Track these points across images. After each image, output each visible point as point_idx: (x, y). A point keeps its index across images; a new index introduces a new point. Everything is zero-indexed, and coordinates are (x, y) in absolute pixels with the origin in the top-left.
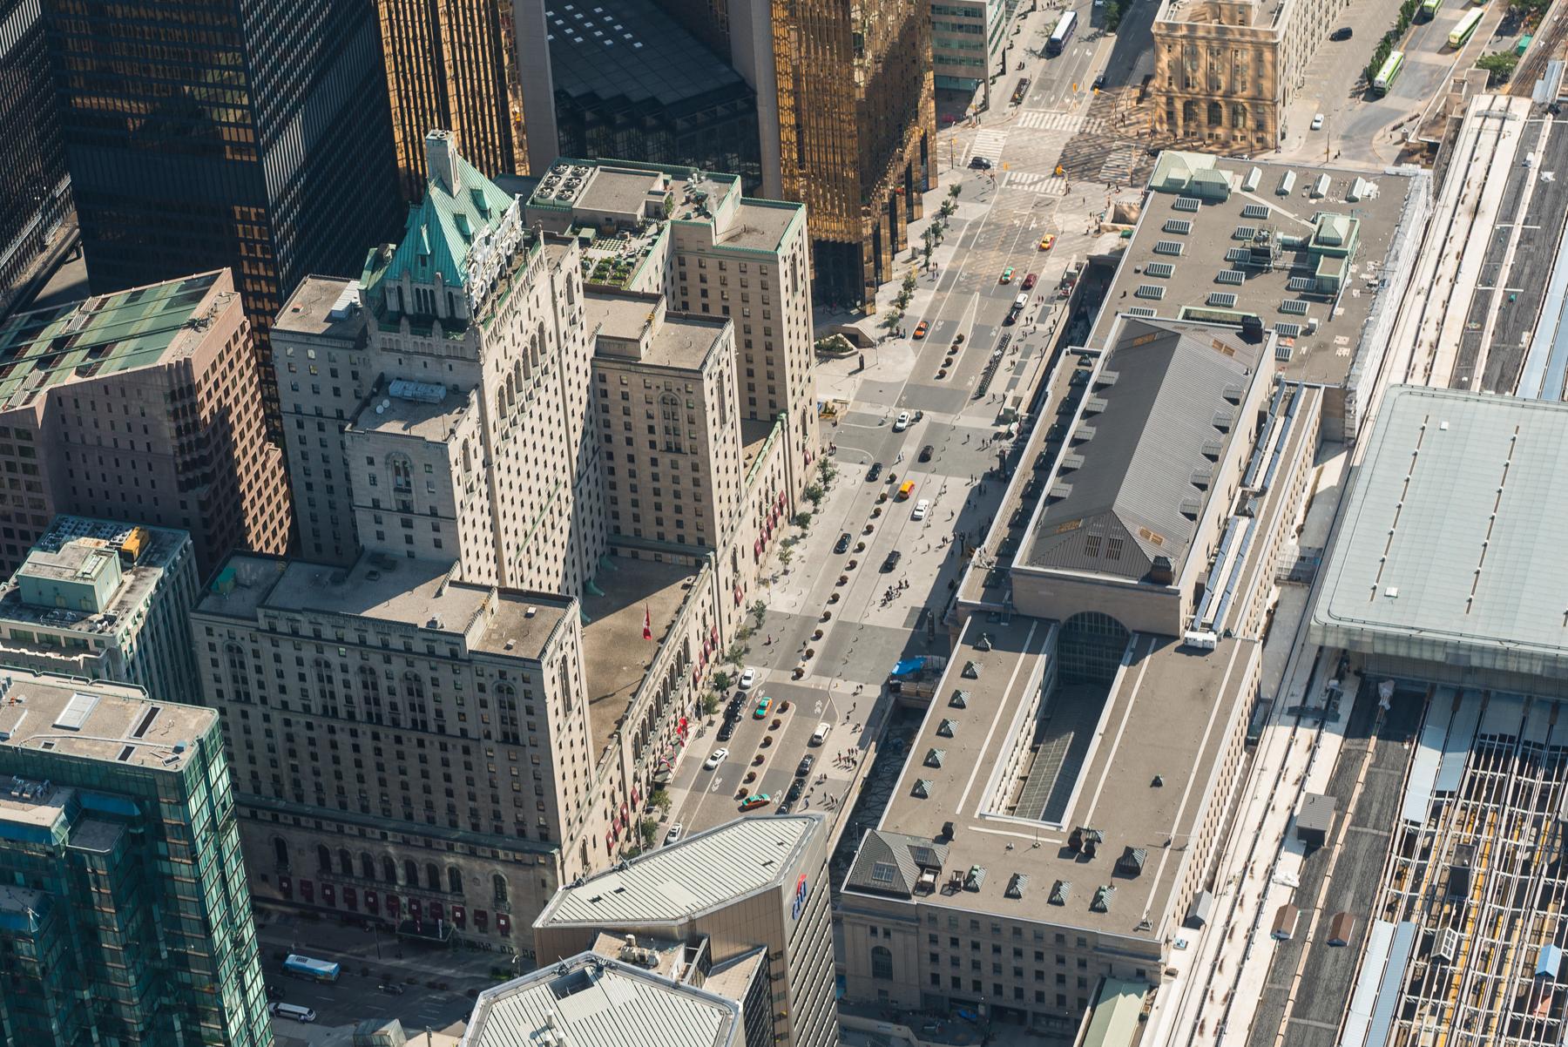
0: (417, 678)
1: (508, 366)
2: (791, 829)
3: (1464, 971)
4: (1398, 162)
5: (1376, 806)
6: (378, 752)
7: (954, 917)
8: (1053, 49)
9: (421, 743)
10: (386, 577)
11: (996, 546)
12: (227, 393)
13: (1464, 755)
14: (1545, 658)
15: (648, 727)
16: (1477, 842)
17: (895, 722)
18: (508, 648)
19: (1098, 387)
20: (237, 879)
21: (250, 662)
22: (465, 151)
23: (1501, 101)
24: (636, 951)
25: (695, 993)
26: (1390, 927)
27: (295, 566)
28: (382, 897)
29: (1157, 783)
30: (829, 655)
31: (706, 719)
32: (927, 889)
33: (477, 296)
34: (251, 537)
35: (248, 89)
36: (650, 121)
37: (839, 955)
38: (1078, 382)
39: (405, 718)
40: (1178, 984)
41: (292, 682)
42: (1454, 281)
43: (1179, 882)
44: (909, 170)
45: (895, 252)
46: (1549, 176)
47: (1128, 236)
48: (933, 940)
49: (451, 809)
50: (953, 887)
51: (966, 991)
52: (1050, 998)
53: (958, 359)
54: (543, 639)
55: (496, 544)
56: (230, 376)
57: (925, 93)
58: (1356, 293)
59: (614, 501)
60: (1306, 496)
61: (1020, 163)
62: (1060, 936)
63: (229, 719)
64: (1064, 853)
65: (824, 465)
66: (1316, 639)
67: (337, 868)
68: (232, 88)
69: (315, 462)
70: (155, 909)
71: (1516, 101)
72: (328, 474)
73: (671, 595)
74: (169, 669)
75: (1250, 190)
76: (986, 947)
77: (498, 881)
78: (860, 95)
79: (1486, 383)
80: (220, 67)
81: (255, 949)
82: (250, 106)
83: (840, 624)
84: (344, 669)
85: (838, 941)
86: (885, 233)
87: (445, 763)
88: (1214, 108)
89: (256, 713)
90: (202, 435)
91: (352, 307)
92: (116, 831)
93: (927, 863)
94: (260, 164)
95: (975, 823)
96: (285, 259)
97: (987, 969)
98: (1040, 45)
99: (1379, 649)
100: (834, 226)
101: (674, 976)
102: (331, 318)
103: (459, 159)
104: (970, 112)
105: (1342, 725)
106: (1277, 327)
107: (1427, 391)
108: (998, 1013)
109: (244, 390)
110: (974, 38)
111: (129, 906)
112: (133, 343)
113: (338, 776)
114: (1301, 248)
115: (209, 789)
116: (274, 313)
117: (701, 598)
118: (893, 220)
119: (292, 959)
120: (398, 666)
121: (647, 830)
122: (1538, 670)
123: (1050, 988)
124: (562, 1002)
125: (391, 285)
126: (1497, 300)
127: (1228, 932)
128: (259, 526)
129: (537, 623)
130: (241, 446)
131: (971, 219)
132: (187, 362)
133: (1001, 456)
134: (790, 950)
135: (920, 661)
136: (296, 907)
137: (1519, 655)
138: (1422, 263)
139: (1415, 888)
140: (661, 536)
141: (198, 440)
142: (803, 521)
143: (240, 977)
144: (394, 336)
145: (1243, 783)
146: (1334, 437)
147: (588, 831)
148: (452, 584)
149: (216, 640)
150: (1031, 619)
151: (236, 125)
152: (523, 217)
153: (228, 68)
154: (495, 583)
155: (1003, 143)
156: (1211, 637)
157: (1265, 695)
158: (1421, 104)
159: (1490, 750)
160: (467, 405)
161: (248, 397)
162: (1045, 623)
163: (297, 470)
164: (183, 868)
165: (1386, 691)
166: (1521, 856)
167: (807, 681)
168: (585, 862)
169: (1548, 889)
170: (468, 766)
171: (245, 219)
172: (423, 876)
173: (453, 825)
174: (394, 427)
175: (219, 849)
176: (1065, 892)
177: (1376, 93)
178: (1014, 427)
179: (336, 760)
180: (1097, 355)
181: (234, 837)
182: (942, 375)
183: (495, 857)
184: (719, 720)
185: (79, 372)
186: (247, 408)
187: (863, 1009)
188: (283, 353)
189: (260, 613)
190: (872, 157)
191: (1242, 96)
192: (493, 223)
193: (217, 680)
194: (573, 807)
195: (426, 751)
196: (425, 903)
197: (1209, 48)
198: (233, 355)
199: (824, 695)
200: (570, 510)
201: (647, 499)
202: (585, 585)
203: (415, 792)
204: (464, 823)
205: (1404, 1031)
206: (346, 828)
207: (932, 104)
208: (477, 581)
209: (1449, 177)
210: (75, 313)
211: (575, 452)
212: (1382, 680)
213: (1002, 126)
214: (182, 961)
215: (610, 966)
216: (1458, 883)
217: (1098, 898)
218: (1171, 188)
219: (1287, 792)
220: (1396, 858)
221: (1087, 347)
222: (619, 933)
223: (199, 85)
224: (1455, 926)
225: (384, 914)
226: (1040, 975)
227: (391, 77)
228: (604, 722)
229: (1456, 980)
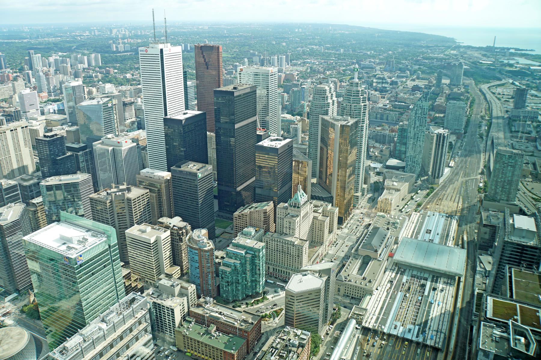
39: (286, 252)
41: (273, 247)
73: (318, 248)
120: (286, 246)
127: (381, 291)
201: (317, 236)
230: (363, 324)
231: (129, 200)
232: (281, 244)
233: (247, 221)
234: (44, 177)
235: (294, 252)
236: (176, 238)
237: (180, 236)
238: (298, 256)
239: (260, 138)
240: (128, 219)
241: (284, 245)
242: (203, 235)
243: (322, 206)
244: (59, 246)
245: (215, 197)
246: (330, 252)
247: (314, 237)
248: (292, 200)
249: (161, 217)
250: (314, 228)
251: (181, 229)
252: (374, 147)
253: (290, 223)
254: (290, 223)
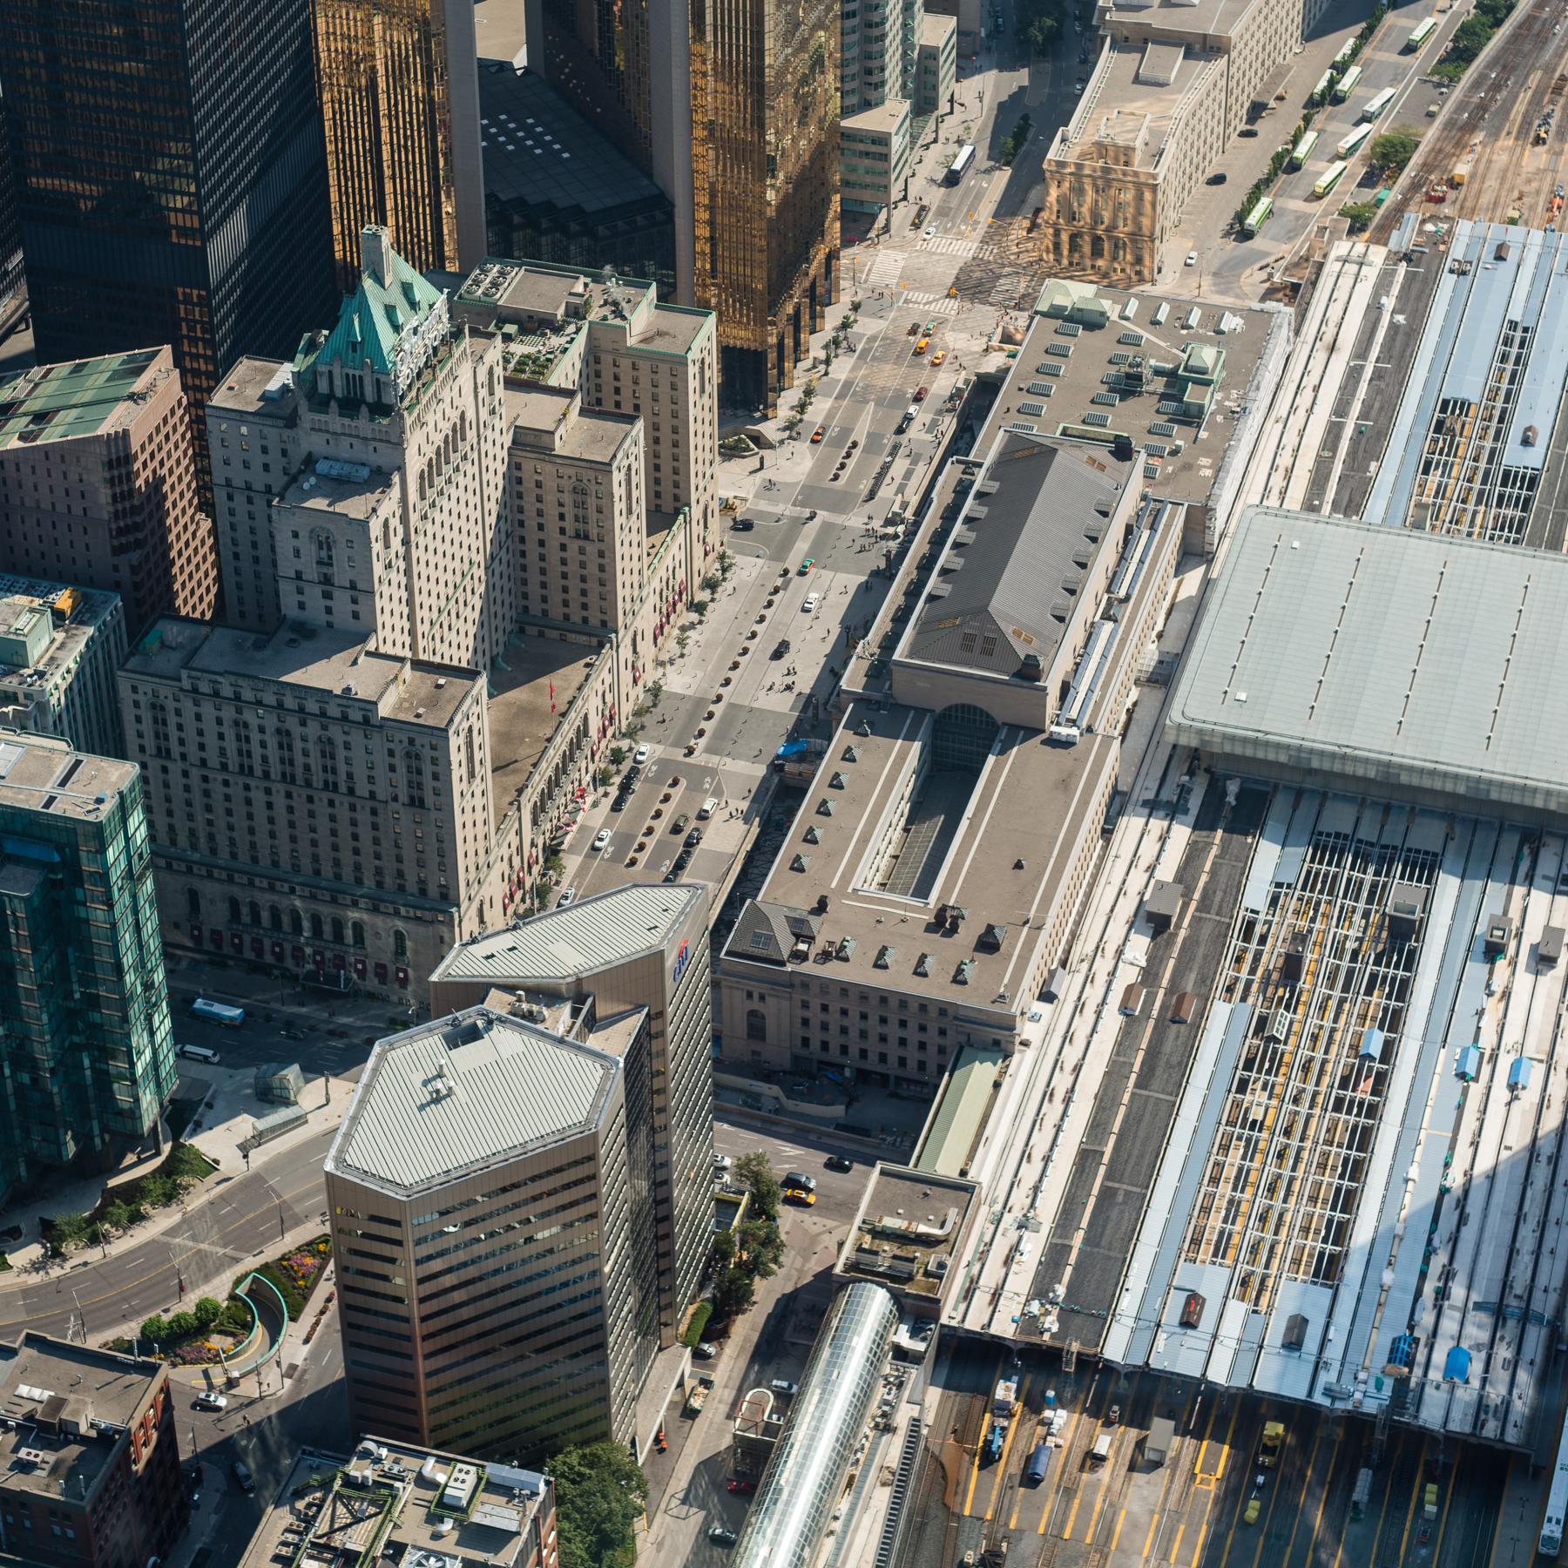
0: (330, 741)
1: (430, 452)
2: (677, 897)
3: (1295, 1051)
4: (1263, 299)
5: (1219, 895)
6: (290, 810)
7: (825, 984)
8: (952, 179)
9: (331, 803)
10: (306, 645)
11: (878, 639)
12: (162, 464)
13: (1302, 850)
14: (1379, 763)
15: (547, 796)
16: (1310, 931)
17: (778, 801)
18: (418, 716)
19: (980, 495)
20: (150, 927)
21: (172, 720)
22: (399, 246)
23: (1360, 248)
24: (525, 1006)
25: (579, 1048)
26: (1228, 1007)
27: (218, 631)
28: (288, 947)
29: (1019, 866)
30: (719, 735)
31: (601, 790)
32: (801, 957)
33: (403, 383)
34: (179, 602)
35: (195, 177)
36: (574, 227)
37: (717, 1016)
38: (962, 490)
39: (318, 778)
40: (1030, 1054)
41: (211, 740)
42: (1310, 411)
43: (1035, 959)
44: (813, 284)
45: (797, 360)
46: (1400, 318)
47: (1014, 356)
48: (805, 1005)
49: (357, 867)
50: (826, 956)
51: (834, 1054)
52: (912, 1064)
53: (851, 464)
54: (451, 709)
55: (411, 617)
56: (166, 449)
57: (831, 214)
58: (1219, 418)
59: (524, 582)
60: (1166, 605)
61: (917, 276)
62: (924, 1005)
63: (149, 773)
64: (930, 928)
65: (722, 557)
66: (1170, 738)
67: (246, 919)
68: (180, 175)
69: (243, 533)
70: (70, 950)
71: (1373, 248)
72: (254, 545)
74: (94, 723)
75: (1127, 319)
76: (854, 1014)
77: (399, 937)
78: (771, 212)
79: (1335, 507)
80: (170, 156)
81: (164, 992)
82: (197, 194)
83: (731, 706)
84: (262, 730)
85: (716, 1004)
86: (789, 342)
87: (354, 823)
88: (1097, 240)
89: (175, 768)
90: (136, 502)
91: (285, 388)
92: (35, 876)
93: (802, 933)
94: (203, 249)
95: (848, 897)
96: (224, 340)
97: (854, 1034)
98: (940, 175)
99: (1228, 749)
100: (742, 333)
101: (560, 1030)
102: (264, 397)
103: (392, 253)
104: (872, 234)
105: (1191, 818)
106: (1146, 447)
107: (1281, 513)
108: (863, 1075)
109: (178, 462)
110: (879, 165)
111: (45, 948)
112: (74, 413)
113: (252, 831)
114: (1171, 375)
115: (127, 839)
116: (210, 390)
117: (602, 678)
118: (797, 330)
119: (199, 1003)
120: (313, 729)
121: (542, 892)
122: (1372, 774)
123: (913, 1055)
124: (454, 1053)
125: (322, 368)
126: (1348, 431)
127: (1079, 1007)
128: (187, 592)
129: (446, 694)
130: (173, 514)
131: (869, 333)
132: (126, 433)
133: (887, 556)
134: (670, 1009)
135: (804, 744)
136: (199, 955)
137: (1356, 759)
138: (1281, 394)
139: (1253, 971)
140: (566, 617)
141: (133, 507)
142: (700, 608)
143: (149, 1018)
144: (323, 417)
145: (1099, 867)
146: (1194, 551)
147: (486, 892)
148: (368, 654)
149: (140, 697)
150: (908, 708)
151: (183, 210)
152: (450, 311)
153: (177, 157)
154: (409, 655)
155: (902, 264)
156: (1074, 731)
157: (1122, 787)
158: (1285, 247)
159: (1326, 845)
160: (389, 486)
161: (181, 469)
162: (921, 712)
163: (225, 540)
164: (98, 913)
165: (1233, 788)
166: (1350, 945)
167: (699, 758)
168: (482, 921)
169: (1373, 977)
170: (375, 827)
171: (187, 300)
172: (327, 929)
173: (359, 881)
174: (320, 503)
175: (134, 897)
176: (930, 963)
177: (1246, 235)
178: (901, 529)
179: (250, 816)
180: (980, 465)
181: (149, 886)
182: (836, 477)
183: (397, 913)
184: (614, 792)
185: (22, 437)
186: (180, 479)
187: (738, 1068)
188: (217, 429)
189: (184, 674)
190: (782, 266)
191: (1122, 231)
192: (422, 314)
193: (140, 735)
194: (472, 869)
195: (335, 811)
196: (329, 955)
197: (1095, 185)
198: (169, 428)
199: (712, 772)
200: (482, 589)
202: (493, 660)
203: (324, 851)
204: (369, 881)
205: (1237, 1105)
206: (257, 881)
207: (838, 225)
208: (391, 652)
209: (1309, 315)
210: (20, 381)
211: (489, 535)
212: (1230, 777)
213: (901, 248)
214: (94, 1002)
215: (500, 1020)
216: (1291, 968)
217: (960, 971)
218: (1055, 313)
219: (1138, 879)
220: (1235, 943)
221: (971, 458)
222: (509, 988)
223: (149, 171)
224: (1287, 1008)
225: (289, 963)
226: (903, 1042)
227: (332, 174)
228: (505, 790)
229: (1286, 1058)
230: (949, 1315)
232: (271, 722)
241: (292, 723)
243: (576, 312)
246: (677, 682)
254: (325, 544)
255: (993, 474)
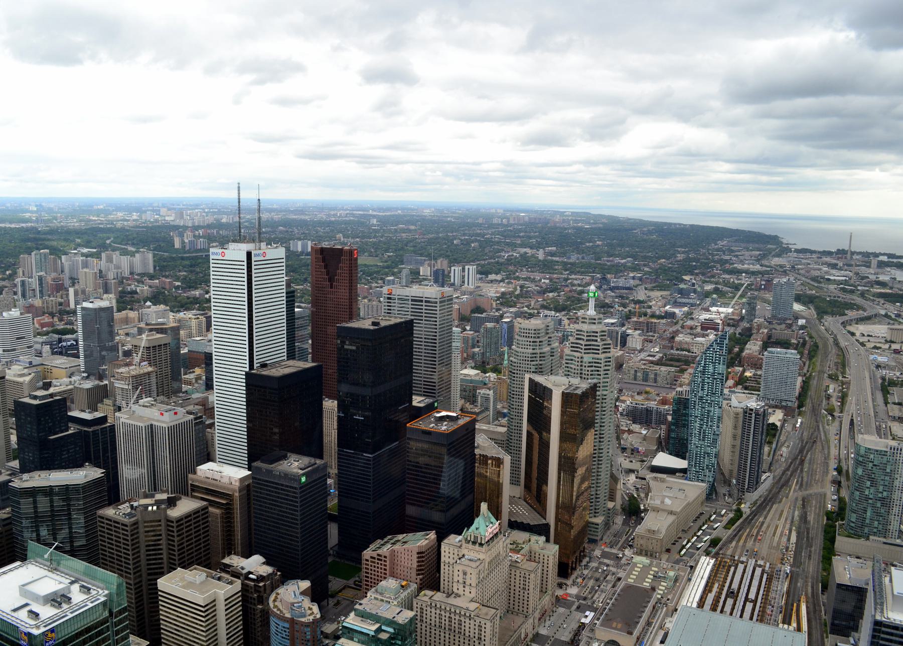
89: (424, 625)
201: (517, 600)
231: (169, 520)
233: (388, 568)
234: (24, 469)
235: (472, 630)
236: (253, 597)
237: (260, 592)
238: (480, 639)
239: (418, 413)
240: (165, 556)
242: (303, 593)
244: (15, 610)
245: (332, 518)
247: (511, 602)
248: (470, 530)
249: (229, 554)
250: (513, 585)
251: (261, 578)
252: (630, 432)
253: (465, 574)
254: (465, 574)
255: (622, 590)
